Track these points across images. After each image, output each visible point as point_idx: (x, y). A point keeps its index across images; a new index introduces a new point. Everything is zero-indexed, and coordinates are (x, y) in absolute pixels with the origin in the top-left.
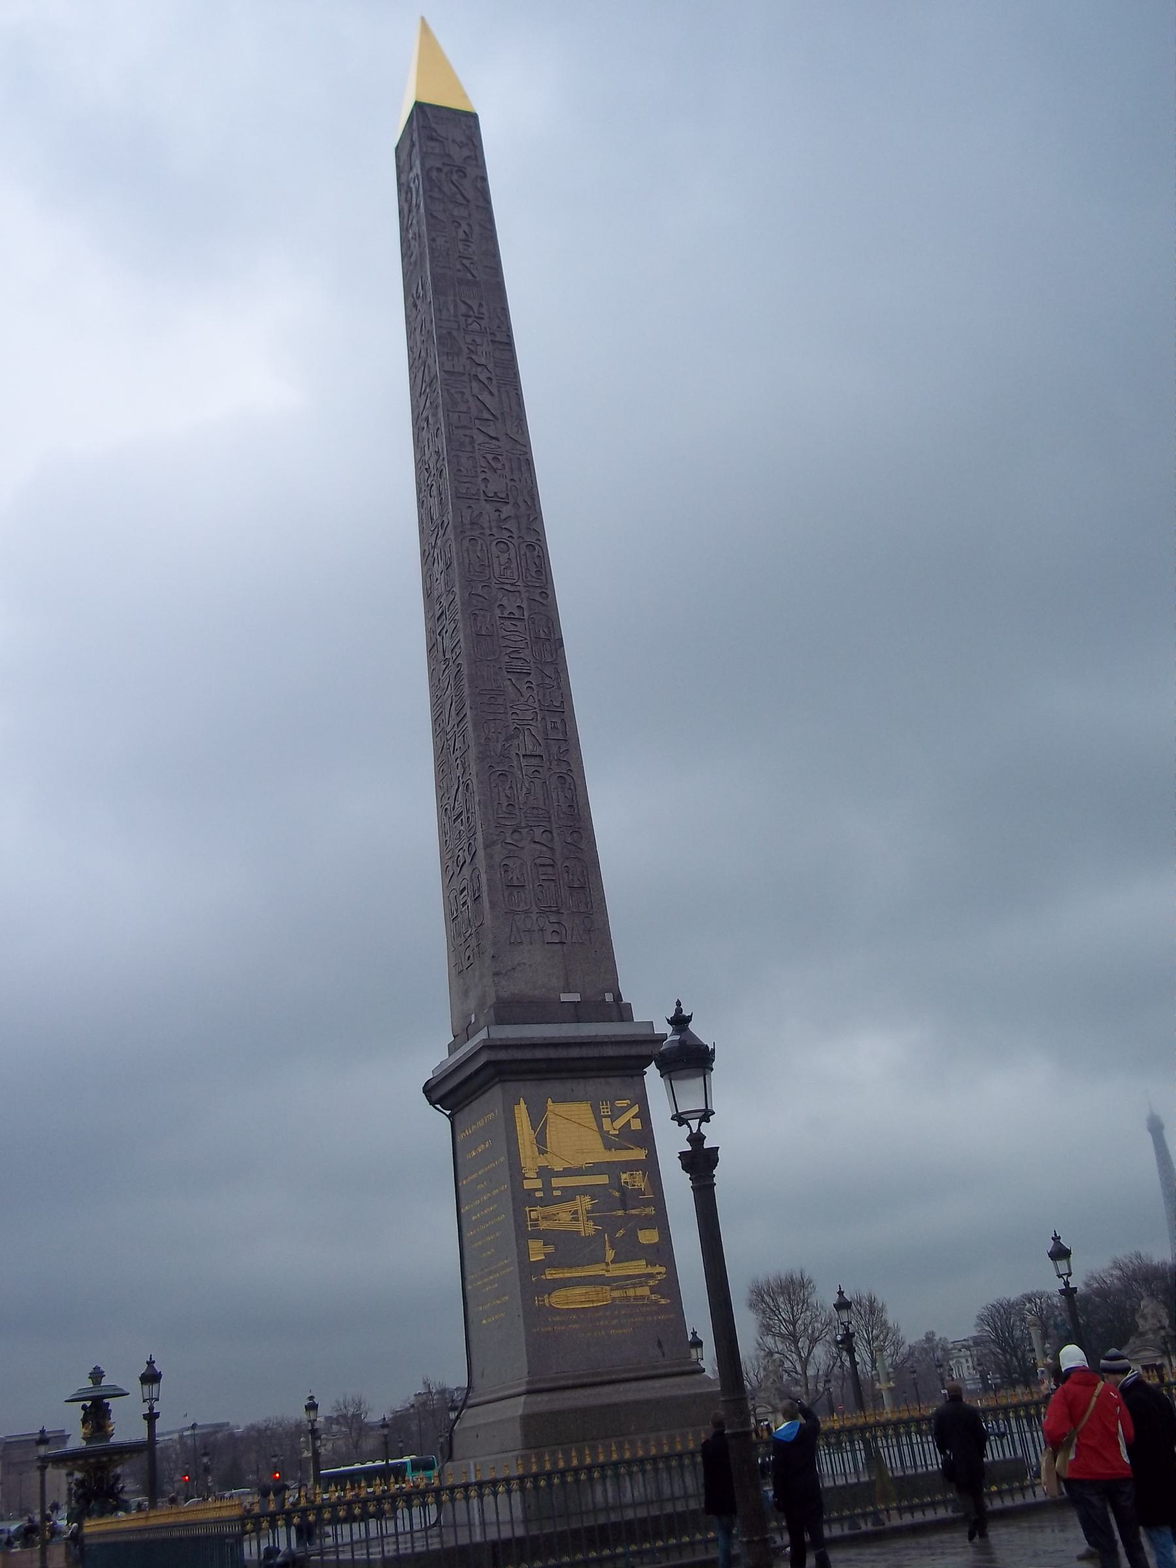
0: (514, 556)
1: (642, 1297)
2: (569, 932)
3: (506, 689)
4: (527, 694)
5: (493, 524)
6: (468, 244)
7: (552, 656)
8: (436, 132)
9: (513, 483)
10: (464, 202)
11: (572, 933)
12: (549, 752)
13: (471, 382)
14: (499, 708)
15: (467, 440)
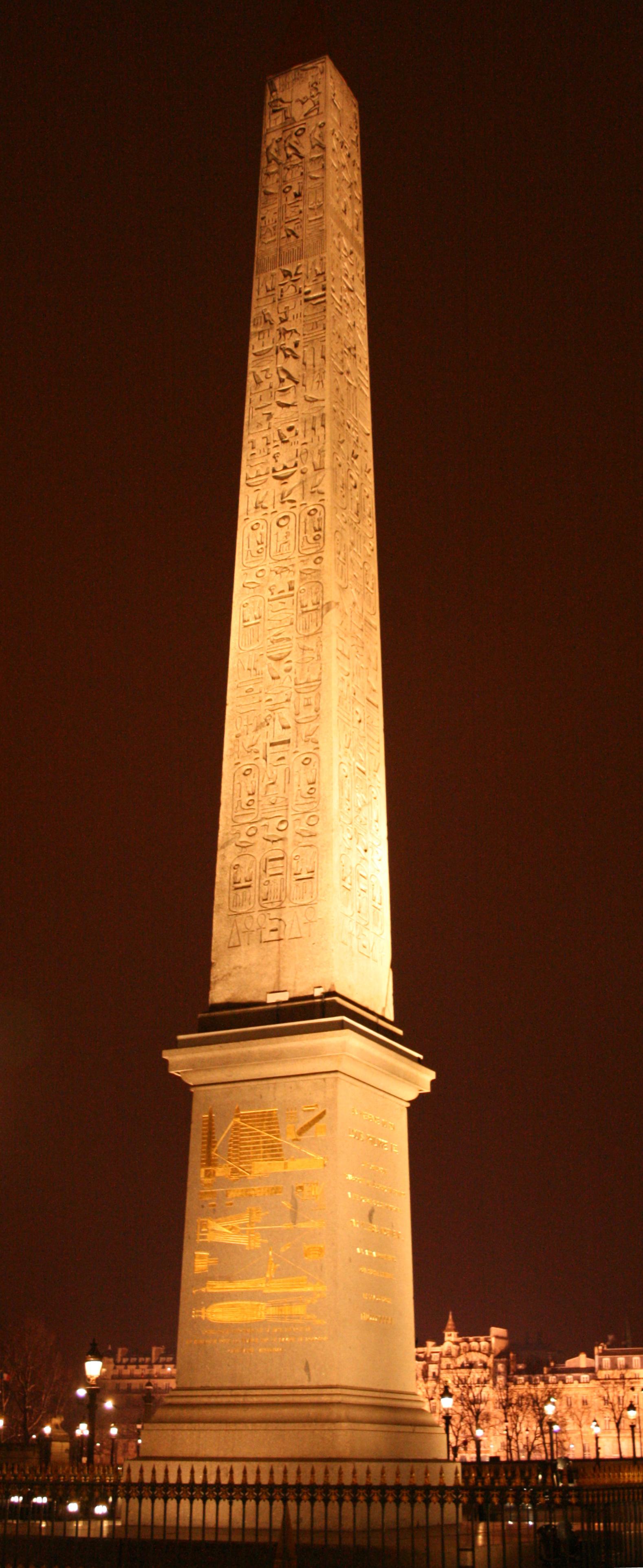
0: (294, 527)
1: (298, 1316)
2: (288, 927)
3: (263, 676)
4: (283, 675)
5: (278, 499)
6: (297, 204)
7: (317, 625)
8: (282, 101)
9: (305, 446)
10: (300, 161)
11: (291, 927)
12: (297, 732)
13: (277, 353)
14: (254, 698)
15: (266, 417)
